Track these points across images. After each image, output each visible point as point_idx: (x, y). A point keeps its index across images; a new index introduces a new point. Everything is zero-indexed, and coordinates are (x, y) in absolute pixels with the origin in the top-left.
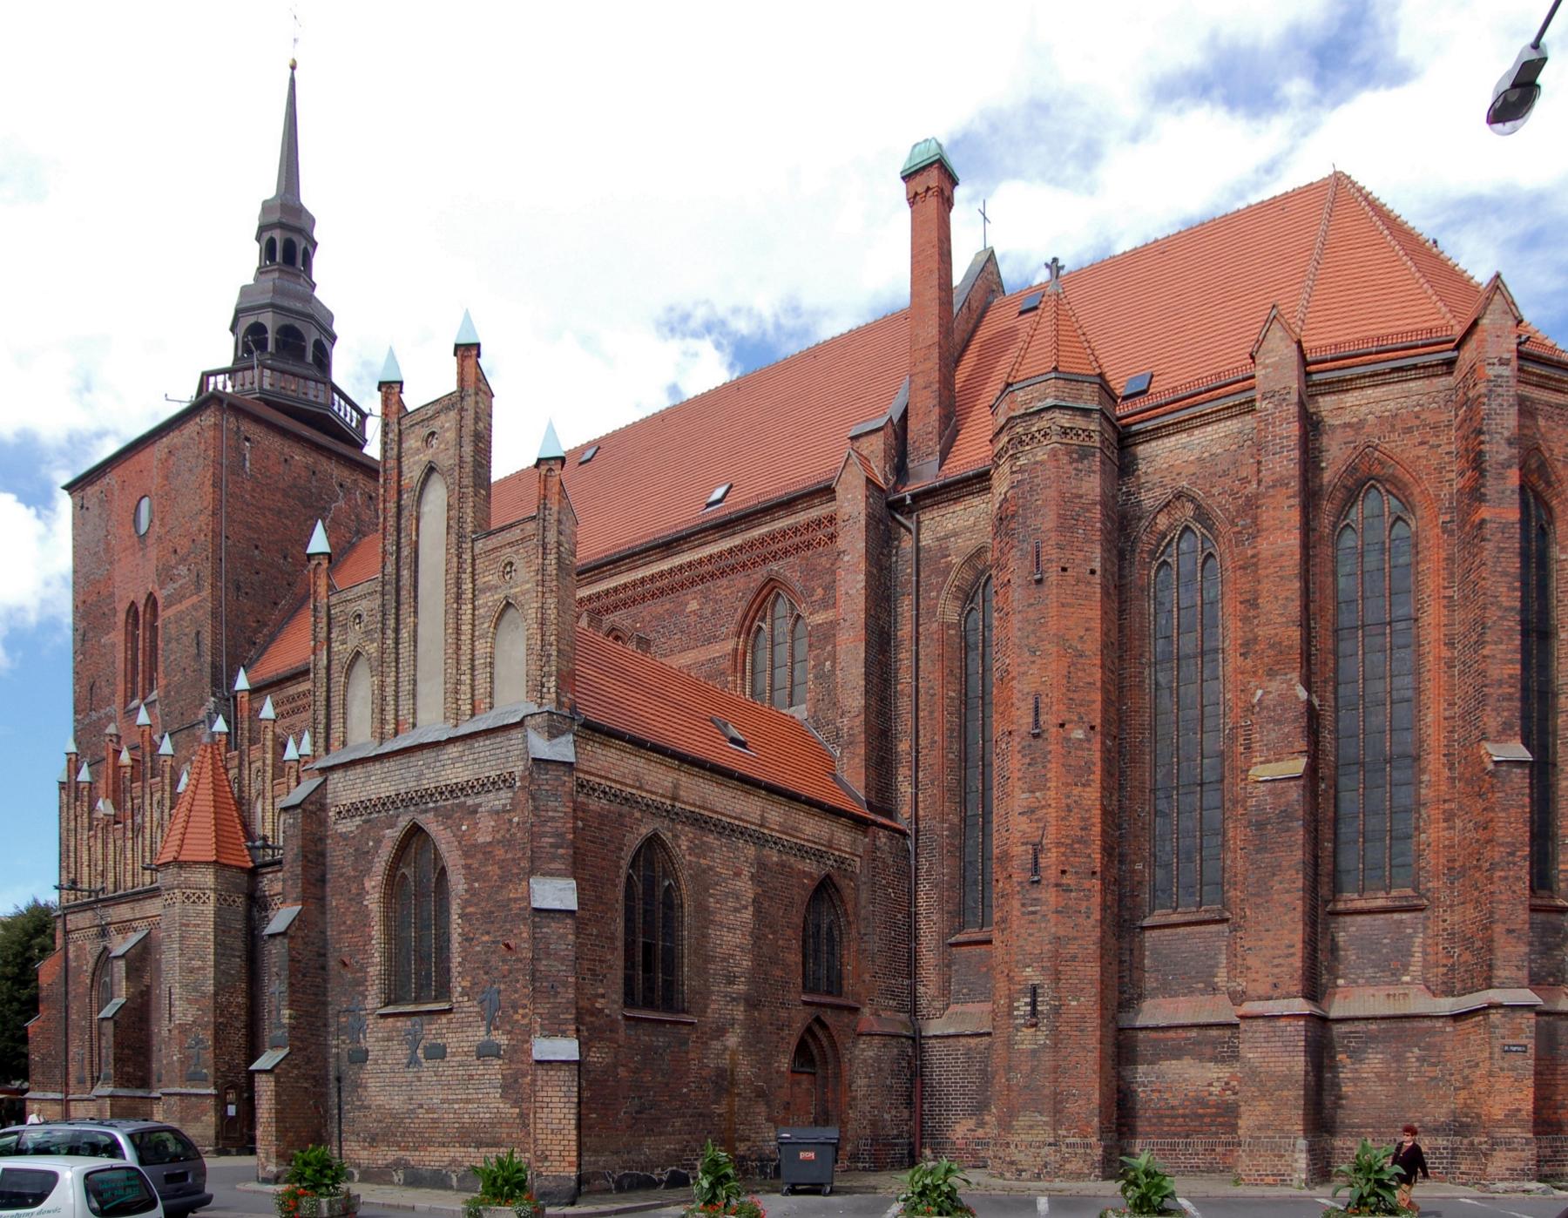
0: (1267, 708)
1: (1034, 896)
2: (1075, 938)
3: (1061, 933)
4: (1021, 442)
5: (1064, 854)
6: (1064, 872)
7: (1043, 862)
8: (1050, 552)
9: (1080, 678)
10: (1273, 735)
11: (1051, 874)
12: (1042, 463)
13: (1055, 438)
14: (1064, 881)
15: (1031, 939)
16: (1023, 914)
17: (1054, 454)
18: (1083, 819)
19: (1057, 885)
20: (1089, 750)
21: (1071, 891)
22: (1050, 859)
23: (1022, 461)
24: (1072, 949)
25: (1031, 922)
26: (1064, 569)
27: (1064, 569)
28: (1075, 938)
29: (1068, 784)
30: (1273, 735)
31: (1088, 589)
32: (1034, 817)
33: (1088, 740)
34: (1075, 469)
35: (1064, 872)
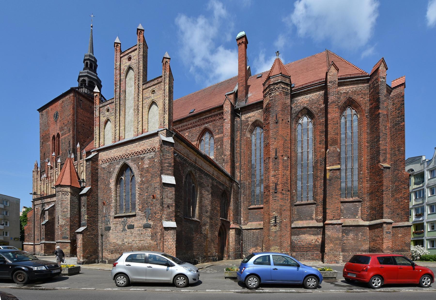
0: (330, 153)
1: (276, 195)
2: (285, 205)
3: (282, 204)
4: (272, 90)
5: (283, 186)
6: (283, 190)
7: (278, 187)
8: (279, 116)
9: (286, 146)
10: (331, 160)
11: (280, 190)
12: (277, 95)
13: (281, 89)
14: (283, 192)
15: (275, 205)
16: (273, 199)
17: (280, 93)
18: (287, 178)
19: (281, 193)
20: (288, 162)
21: (284, 194)
22: (279, 187)
23: (273, 95)
24: (284, 208)
25: (275, 201)
26: (283, 120)
27: (283, 120)
28: (285, 205)
29: (283, 170)
30: (331, 160)
31: (288, 125)
32: (275, 177)
33: (288, 160)
34: (285, 97)
35: (283, 190)
